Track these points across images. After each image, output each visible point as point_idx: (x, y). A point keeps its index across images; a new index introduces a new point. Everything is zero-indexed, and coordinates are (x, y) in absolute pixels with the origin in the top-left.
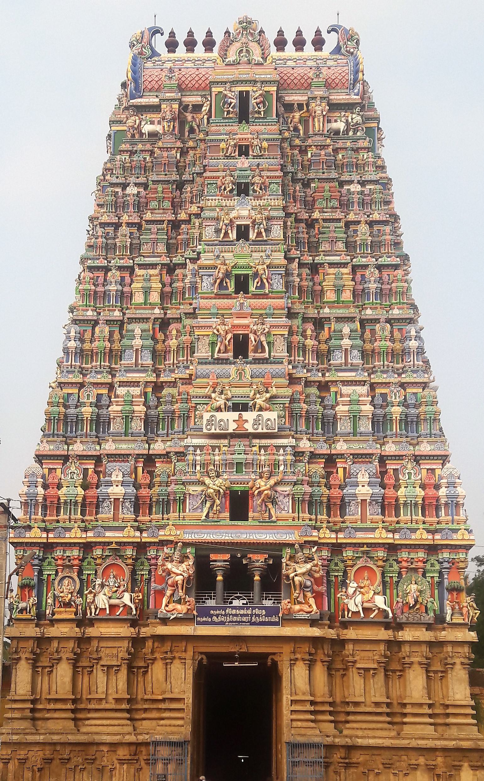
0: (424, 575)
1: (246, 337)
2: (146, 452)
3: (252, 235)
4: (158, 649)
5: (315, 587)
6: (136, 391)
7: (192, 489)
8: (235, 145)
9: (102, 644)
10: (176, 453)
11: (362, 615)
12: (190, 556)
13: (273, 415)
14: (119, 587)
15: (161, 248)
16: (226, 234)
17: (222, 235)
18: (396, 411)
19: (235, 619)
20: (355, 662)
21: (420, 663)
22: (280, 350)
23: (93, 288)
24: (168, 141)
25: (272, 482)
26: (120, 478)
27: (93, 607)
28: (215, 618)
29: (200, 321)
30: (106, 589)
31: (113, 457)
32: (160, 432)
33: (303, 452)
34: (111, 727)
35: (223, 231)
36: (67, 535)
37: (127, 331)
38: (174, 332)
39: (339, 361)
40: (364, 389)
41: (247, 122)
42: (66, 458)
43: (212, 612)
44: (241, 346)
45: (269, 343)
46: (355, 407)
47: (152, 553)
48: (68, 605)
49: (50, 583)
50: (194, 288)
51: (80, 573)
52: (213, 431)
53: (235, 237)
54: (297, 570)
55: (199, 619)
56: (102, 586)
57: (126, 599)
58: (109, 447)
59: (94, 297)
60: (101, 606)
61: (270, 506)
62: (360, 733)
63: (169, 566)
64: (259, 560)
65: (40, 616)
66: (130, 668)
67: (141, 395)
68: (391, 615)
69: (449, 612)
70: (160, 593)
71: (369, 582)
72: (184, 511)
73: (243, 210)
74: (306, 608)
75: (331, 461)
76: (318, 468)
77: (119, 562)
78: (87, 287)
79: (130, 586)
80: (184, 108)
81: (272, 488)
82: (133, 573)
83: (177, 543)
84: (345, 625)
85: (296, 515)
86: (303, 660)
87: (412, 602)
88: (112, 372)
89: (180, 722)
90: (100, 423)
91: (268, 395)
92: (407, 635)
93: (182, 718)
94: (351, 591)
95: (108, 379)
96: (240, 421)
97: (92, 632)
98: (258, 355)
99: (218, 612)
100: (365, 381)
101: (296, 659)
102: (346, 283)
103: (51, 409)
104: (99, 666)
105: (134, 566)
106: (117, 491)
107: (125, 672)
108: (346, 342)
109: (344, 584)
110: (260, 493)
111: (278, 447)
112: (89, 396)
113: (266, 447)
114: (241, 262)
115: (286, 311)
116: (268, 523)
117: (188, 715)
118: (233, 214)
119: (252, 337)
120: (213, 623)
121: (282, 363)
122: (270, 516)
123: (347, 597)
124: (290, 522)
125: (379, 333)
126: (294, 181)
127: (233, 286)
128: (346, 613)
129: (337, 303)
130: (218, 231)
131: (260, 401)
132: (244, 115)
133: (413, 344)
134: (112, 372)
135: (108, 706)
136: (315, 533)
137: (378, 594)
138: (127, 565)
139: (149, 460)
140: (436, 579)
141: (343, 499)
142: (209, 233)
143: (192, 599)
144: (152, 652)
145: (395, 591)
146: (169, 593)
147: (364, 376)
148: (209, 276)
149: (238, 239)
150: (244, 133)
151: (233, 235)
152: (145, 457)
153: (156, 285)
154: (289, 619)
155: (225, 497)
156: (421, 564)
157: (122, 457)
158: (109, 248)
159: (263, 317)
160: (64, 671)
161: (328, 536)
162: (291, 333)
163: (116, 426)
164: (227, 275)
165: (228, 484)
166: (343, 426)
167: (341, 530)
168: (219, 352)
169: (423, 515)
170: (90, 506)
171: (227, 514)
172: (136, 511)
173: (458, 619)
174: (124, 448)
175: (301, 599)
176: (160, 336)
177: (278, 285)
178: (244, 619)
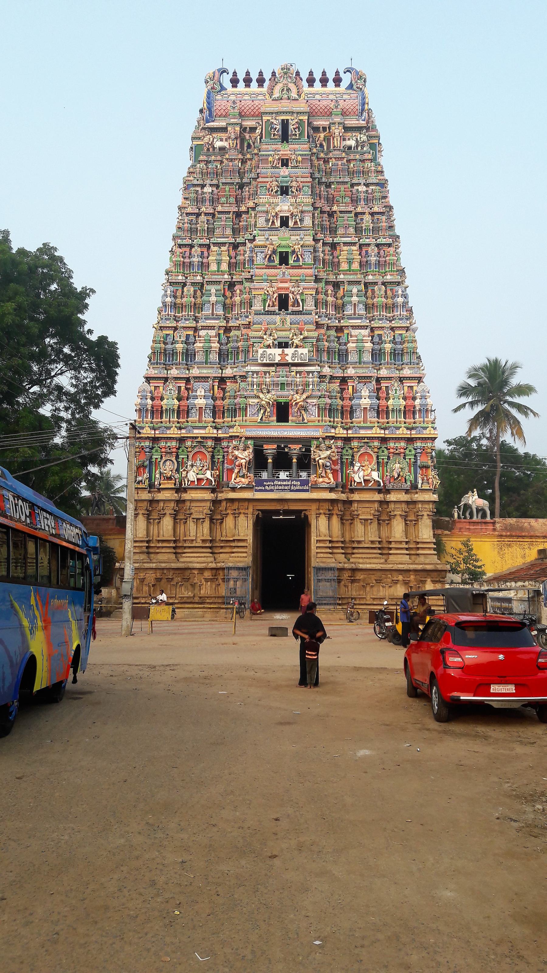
0: (405, 458)
1: (287, 296)
2: (220, 375)
3: (291, 224)
4: (230, 508)
5: (333, 466)
6: (213, 333)
7: (252, 401)
8: (279, 159)
9: (192, 505)
10: (240, 376)
11: (363, 484)
12: (250, 446)
13: (305, 351)
14: (203, 467)
15: (229, 232)
16: (273, 222)
17: (270, 224)
18: (388, 347)
19: (280, 488)
20: (358, 515)
21: (401, 516)
22: (310, 305)
23: (182, 260)
24: (232, 154)
25: (304, 396)
26: (203, 394)
27: (186, 480)
28: (267, 487)
29: (256, 285)
30: (195, 468)
31: (198, 379)
32: (230, 361)
33: (325, 376)
34: (200, 558)
35: (271, 221)
36: (168, 432)
37: (206, 291)
38: (238, 291)
39: (350, 312)
40: (366, 332)
41: (287, 142)
42: (166, 379)
43: (265, 483)
44: (283, 302)
45: (302, 300)
46: (360, 345)
47: (225, 444)
48: (169, 478)
49: (157, 464)
51: (177, 457)
52: (265, 361)
53: (279, 225)
54: (321, 455)
55: (256, 488)
56: (192, 466)
57: (208, 474)
58: (195, 372)
59: (184, 266)
60: (191, 479)
61: (303, 412)
62: (361, 561)
63: (236, 453)
64: (295, 449)
65: (151, 486)
66: (211, 520)
67: (216, 336)
68: (382, 484)
69: (420, 482)
70: (231, 471)
71: (368, 462)
72: (246, 416)
73: (284, 206)
74: (327, 480)
75: (344, 380)
76: (335, 386)
77: (203, 450)
78: (178, 259)
79: (210, 466)
80: (244, 129)
81: (304, 400)
82: (213, 457)
83: (241, 438)
84: (352, 491)
85: (320, 418)
86: (325, 514)
87: (396, 476)
88: (196, 319)
89: (245, 555)
90: (189, 355)
91: (302, 337)
92: (392, 497)
93: (246, 552)
94: (356, 468)
95: (193, 324)
96: (283, 355)
97: (186, 496)
98: (295, 309)
99: (269, 483)
100: (367, 326)
101: (320, 514)
102: (355, 257)
103: (155, 345)
104: (190, 519)
105: (213, 452)
106: (201, 402)
107: (209, 522)
108: (355, 299)
109: (352, 465)
110: (296, 404)
111: (308, 373)
113: (300, 373)
114: (284, 243)
115: (314, 278)
116: (302, 424)
117: (250, 550)
118: (278, 209)
119: (291, 296)
120: (266, 491)
121: (311, 314)
122: (303, 419)
123: (354, 472)
124: (317, 423)
125: (377, 292)
126: (319, 183)
127: (278, 260)
128: (353, 483)
129: (349, 271)
130: (267, 221)
131: (296, 341)
132: (285, 137)
133: (400, 300)
134: (196, 319)
135: (197, 545)
136: (333, 431)
137: (374, 470)
138: (208, 452)
139: (222, 380)
140: (413, 460)
141: (351, 407)
142: (261, 222)
143: (252, 475)
144: (226, 509)
145: (385, 468)
146: (236, 471)
147: (366, 323)
148: (262, 252)
149: (281, 227)
150: (285, 150)
151: (278, 224)
152: (219, 378)
154: (316, 487)
155: (273, 407)
156: (402, 451)
157: (205, 379)
158: (193, 231)
159: (299, 282)
160: (167, 522)
161: (342, 433)
162: (317, 293)
163: (199, 358)
164: (274, 252)
165: (275, 397)
166: (353, 358)
167: (350, 428)
168: (269, 306)
169: (405, 418)
170: (183, 412)
171: (275, 418)
172: (214, 417)
173: (426, 487)
174: (205, 372)
175: (323, 474)
176: (228, 294)
177: (309, 259)
178: (286, 488)
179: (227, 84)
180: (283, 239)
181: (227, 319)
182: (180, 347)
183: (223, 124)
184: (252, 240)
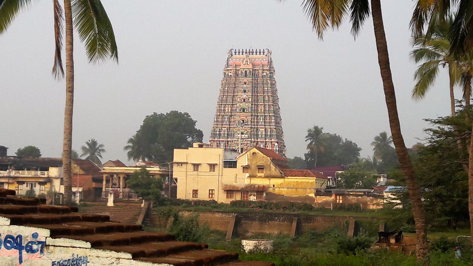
6: (226, 129)
13: (247, 135)
15: (231, 101)
18: (269, 133)
40: (263, 129)
50: (236, 110)
58: (221, 139)
59: (219, 111)
73: (244, 96)
76: (255, 144)
90: (220, 135)
108: (261, 120)
112: (218, 130)
142: (239, 100)
151: (243, 101)
153: (230, 109)
157: (223, 141)
158: (222, 100)
159: (247, 117)
163: (222, 135)
174: (224, 139)
177: (250, 111)
180: (243, 105)
181: (229, 125)
182: (218, 133)
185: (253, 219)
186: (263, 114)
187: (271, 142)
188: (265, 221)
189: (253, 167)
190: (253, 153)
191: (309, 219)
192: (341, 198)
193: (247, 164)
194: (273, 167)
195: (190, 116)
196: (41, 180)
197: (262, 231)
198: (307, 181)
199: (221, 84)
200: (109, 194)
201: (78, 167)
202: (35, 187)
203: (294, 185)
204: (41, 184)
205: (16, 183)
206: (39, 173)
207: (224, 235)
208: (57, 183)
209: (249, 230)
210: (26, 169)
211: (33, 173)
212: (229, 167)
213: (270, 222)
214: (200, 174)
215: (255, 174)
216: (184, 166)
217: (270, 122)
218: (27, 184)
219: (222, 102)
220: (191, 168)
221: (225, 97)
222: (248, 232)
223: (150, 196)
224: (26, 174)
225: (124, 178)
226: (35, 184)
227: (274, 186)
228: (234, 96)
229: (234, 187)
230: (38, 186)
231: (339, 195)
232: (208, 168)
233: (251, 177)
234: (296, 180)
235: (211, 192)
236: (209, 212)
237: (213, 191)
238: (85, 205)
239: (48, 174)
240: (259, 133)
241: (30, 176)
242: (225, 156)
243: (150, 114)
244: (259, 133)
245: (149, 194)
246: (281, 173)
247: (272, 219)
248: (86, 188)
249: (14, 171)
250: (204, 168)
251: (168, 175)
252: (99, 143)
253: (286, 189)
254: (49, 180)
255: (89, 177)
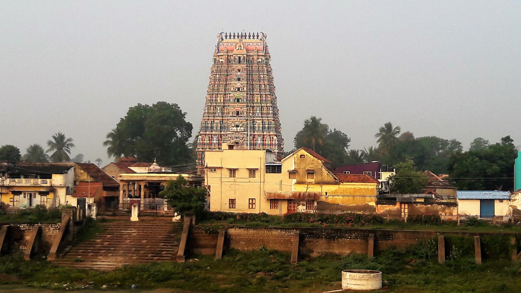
6: (218, 121)
13: (243, 128)
15: (224, 90)
18: (267, 126)
24: (225, 65)
40: (261, 121)
44: (238, 113)
50: (230, 100)
58: (214, 133)
73: (238, 85)
80: (228, 56)
90: (212, 127)
106: (215, 142)
108: (258, 112)
112: (209, 122)
126: (249, 74)
142: (232, 89)
147: (261, 118)
150: (239, 66)
151: (237, 90)
153: (222, 99)
157: (216, 135)
159: (241, 107)
163: (215, 129)
177: (245, 101)
179: (224, 38)
180: (238, 95)
181: (222, 117)
182: (209, 125)
183: (222, 54)
184: (230, 94)
185: (318, 237)
186: (260, 105)
187: (270, 135)
188: (334, 238)
189: (301, 172)
190: (301, 156)
191: (387, 235)
192: (406, 206)
193: (293, 169)
194: (325, 172)
195: (179, 108)
196: (42, 190)
197: (330, 251)
198: (366, 187)
199: (210, 71)
200: (133, 207)
201: (86, 174)
202: (35, 197)
203: (350, 192)
204: (42, 194)
205: (11, 193)
206: (39, 181)
207: (287, 256)
208: (62, 193)
209: (314, 250)
210: (22, 177)
211: (32, 182)
212: (272, 173)
213: (340, 240)
214: (237, 180)
215: (303, 180)
216: (218, 171)
217: (267, 114)
218: (25, 194)
219: (213, 91)
220: (227, 173)
221: (216, 85)
222: (313, 252)
223: (192, 211)
224: (23, 182)
225: (145, 187)
226: (35, 194)
227: (326, 193)
228: (226, 84)
229: (279, 195)
230: (38, 197)
231: (405, 203)
232: (247, 173)
233: (298, 183)
234: (353, 187)
235: (252, 202)
236: (265, 228)
237: (254, 200)
238: (104, 220)
239: (51, 182)
240: (256, 125)
241: (28, 185)
242: (266, 159)
243: (134, 104)
244: (256, 125)
245: (190, 208)
246: (335, 179)
247: (341, 237)
248: (98, 199)
249: (8, 180)
250: (243, 174)
251: (199, 182)
252: (67, 137)
253: (341, 197)
254: (52, 190)
255: (100, 185)
